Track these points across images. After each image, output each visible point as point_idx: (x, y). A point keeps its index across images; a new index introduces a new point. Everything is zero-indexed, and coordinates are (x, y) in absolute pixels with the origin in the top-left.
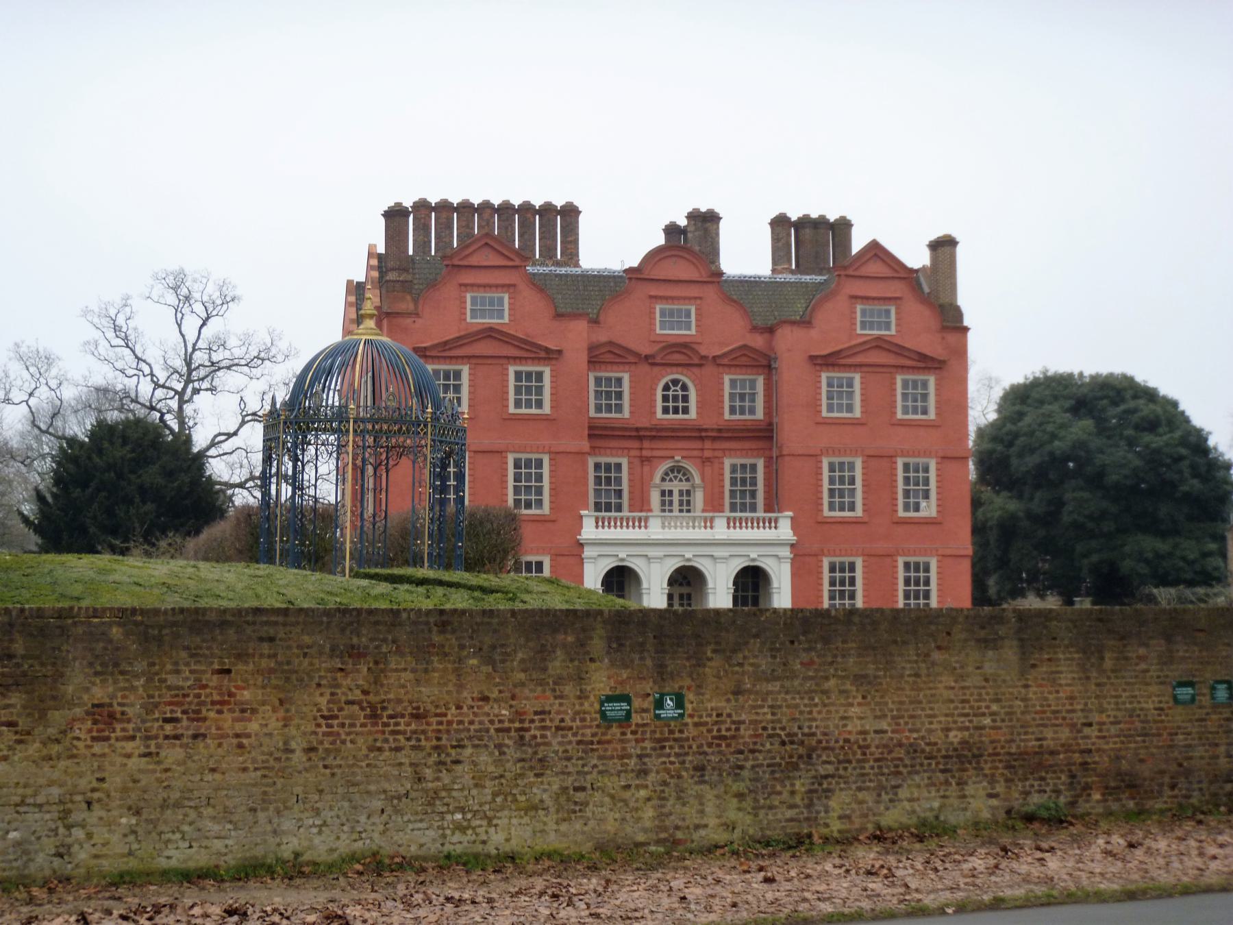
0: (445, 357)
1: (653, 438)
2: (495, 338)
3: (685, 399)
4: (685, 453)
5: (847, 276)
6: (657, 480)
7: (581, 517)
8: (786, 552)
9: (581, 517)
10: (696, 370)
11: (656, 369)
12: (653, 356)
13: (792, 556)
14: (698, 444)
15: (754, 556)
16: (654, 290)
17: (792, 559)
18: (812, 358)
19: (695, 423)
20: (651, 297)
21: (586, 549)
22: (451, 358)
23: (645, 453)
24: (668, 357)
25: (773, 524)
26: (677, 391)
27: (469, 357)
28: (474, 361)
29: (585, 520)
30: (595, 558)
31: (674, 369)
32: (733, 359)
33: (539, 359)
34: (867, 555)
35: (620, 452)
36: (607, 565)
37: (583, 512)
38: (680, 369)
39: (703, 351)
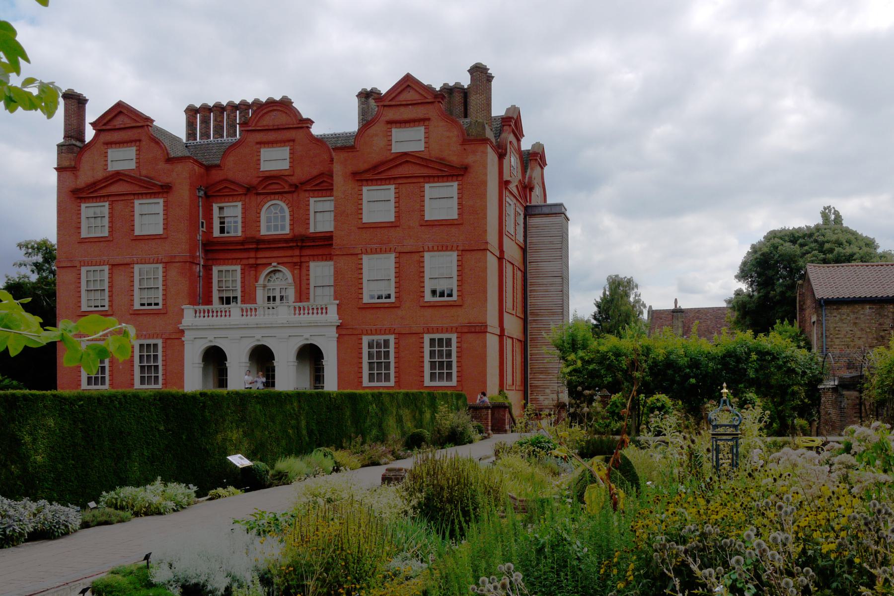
0: (93, 197)
1: (257, 250)
2: (125, 181)
3: (283, 218)
4: (280, 260)
5: (384, 106)
6: (261, 281)
7: (183, 310)
8: (333, 333)
9: (183, 310)
10: (289, 196)
11: (259, 198)
12: (255, 188)
13: (337, 335)
14: (289, 253)
15: (308, 337)
16: (259, 137)
17: (338, 338)
18: (355, 174)
19: (288, 237)
20: (258, 143)
21: (186, 333)
22: (96, 197)
23: (252, 261)
24: (271, 187)
25: (324, 311)
26: (276, 213)
27: (108, 196)
28: (110, 199)
29: (186, 312)
30: (192, 341)
31: (272, 197)
32: (317, 185)
33: (155, 193)
34: (399, 335)
35: (234, 261)
36: (203, 345)
37: (183, 307)
38: (277, 197)
39: (294, 180)
